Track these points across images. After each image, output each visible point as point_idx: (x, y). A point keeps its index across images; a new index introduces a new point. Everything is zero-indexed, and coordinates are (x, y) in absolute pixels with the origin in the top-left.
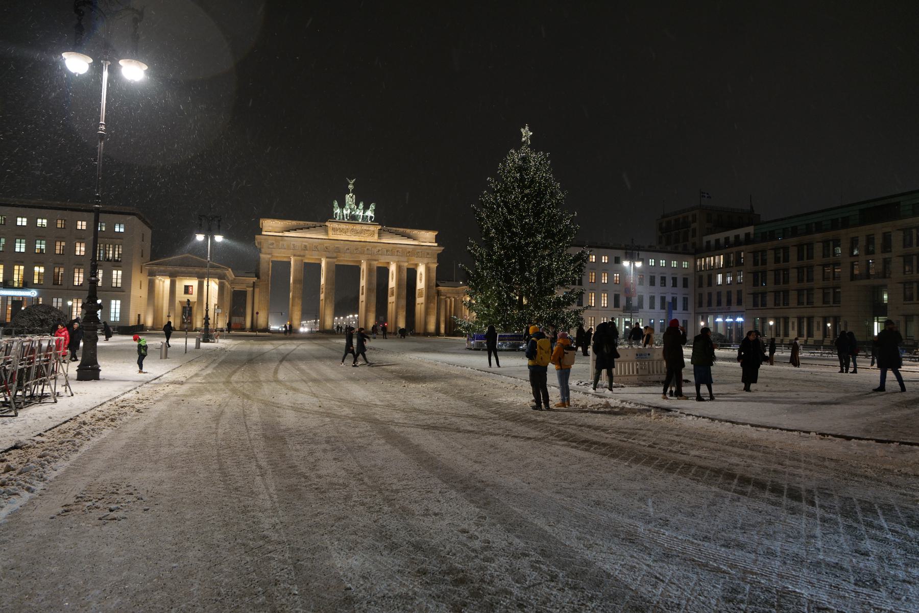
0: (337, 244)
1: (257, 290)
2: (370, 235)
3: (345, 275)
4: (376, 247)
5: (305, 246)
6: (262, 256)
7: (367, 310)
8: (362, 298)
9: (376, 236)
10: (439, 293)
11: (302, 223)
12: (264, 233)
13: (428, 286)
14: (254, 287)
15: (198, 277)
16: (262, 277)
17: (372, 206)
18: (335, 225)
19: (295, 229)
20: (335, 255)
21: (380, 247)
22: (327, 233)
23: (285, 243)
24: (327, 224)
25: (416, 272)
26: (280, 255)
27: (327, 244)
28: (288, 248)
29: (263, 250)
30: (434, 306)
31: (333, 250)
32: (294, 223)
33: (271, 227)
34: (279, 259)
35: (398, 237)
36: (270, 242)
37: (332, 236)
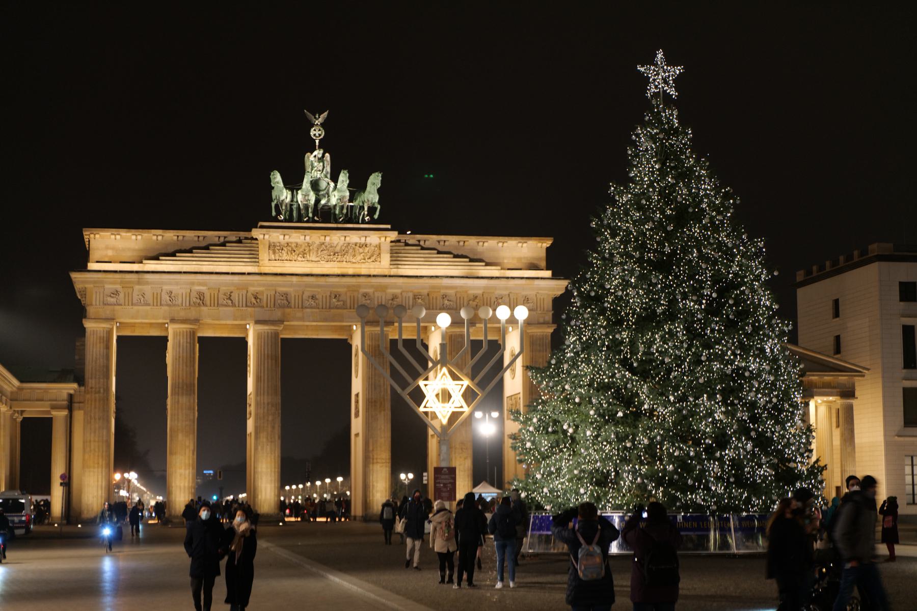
0: (283, 286)
1: (79, 415)
2: (368, 256)
3: (311, 371)
4: (383, 288)
5: (201, 296)
6: (88, 325)
7: (367, 460)
8: (357, 425)
9: (386, 259)
11: (190, 235)
12: (92, 266)
16: (91, 382)
17: (375, 181)
18: (277, 236)
20: (278, 314)
21: (396, 287)
22: (254, 256)
23: (147, 289)
24: (256, 233)
26: (141, 321)
27: (257, 285)
28: (157, 301)
29: (91, 311)
31: (275, 305)
32: (170, 236)
34: (138, 333)
36: (109, 287)
37: (268, 263)
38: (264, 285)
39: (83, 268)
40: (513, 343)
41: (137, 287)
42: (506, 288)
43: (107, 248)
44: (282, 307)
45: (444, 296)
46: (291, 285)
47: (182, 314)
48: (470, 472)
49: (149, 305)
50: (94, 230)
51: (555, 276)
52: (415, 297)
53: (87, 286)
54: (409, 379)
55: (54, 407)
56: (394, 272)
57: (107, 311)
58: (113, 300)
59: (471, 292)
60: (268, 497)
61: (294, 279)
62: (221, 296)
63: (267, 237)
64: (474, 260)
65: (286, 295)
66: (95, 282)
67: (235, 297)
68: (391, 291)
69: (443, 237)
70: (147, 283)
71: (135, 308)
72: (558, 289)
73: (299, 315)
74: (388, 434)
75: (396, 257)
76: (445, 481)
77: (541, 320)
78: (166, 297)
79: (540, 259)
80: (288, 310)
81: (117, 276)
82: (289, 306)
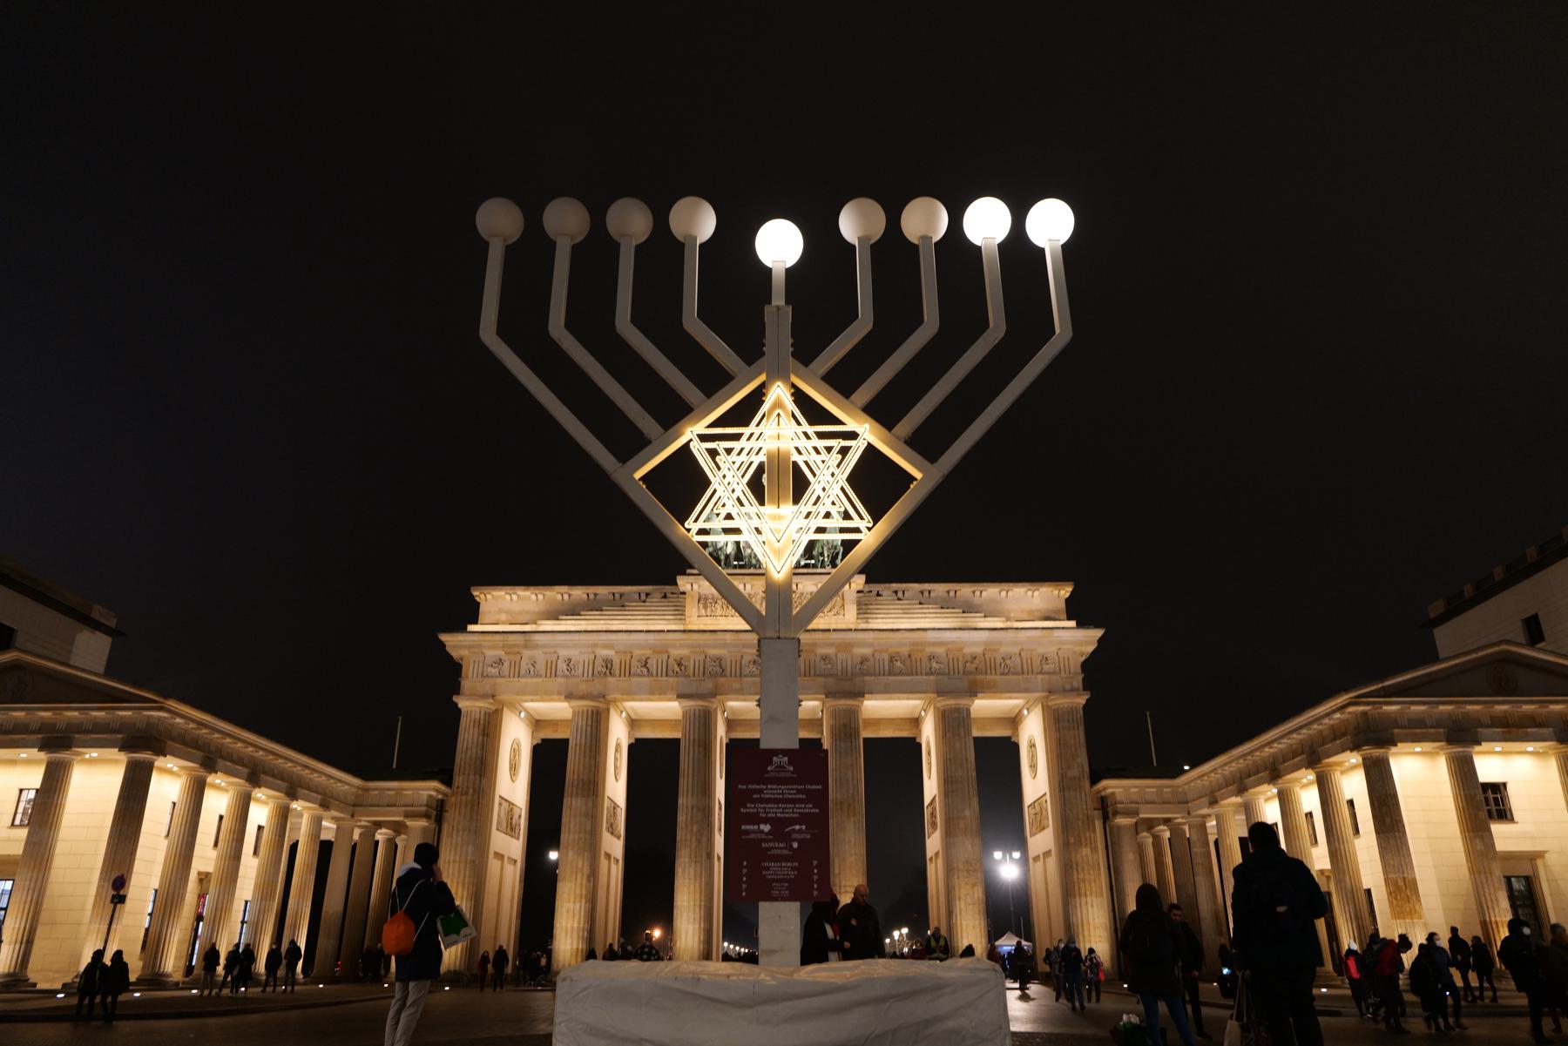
1: (446, 827)
4: (846, 647)
5: (608, 664)
6: (463, 703)
10: (1106, 808)
11: (603, 591)
13: (1062, 784)
14: (439, 821)
15: (44, 746)
16: (458, 780)
19: (573, 611)
20: (709, 685)
22: (680, 612)
23: (538, 654)
25: (1016, 747)
28: (551, 670)
29: (466, 684)
30: (1092, 857)
32: (579, 593)
33: (504, 608)
35: (931, 609)
36: (490, 653)
38: (688, 646)
39: (463, 630)
40: (1033, 732)
41: (526, 653)
42: (1015, 643)
43: (500, 611)
44: (713, 675)
45: (931, 658)
46: (724, 646)
47: (583, 688)
48: (982, 906)
49: (538, 675)
50: (486, 589)
51: (1080, 625)
52: (891, 659)
53: (465, 653)
54: (646, 423)
55: (407, 815)
56: (863, 626)
57: (486, 686)
58: (494, 671)
59: (968, 650)
60: (690, 943)
61: (728, 636)
62: (634, 662)
63: (695, 587)
64: (969, 608)
65: (719, 661)
66: (470, 647)
67: (652, 664)
68: (860, 651)
69: (927, 586)
70: (536, 646)
71: (523, 680)
72: (1088, 643)
73: (737, 686)
74: (863, 851)
75: (863, 608)
76: (775, 811)
77: (1068, 687)
78: (562, 666)
79: (1058, 611)
80: (722, 680)
81: (498, 637)
82: (723, 673)
